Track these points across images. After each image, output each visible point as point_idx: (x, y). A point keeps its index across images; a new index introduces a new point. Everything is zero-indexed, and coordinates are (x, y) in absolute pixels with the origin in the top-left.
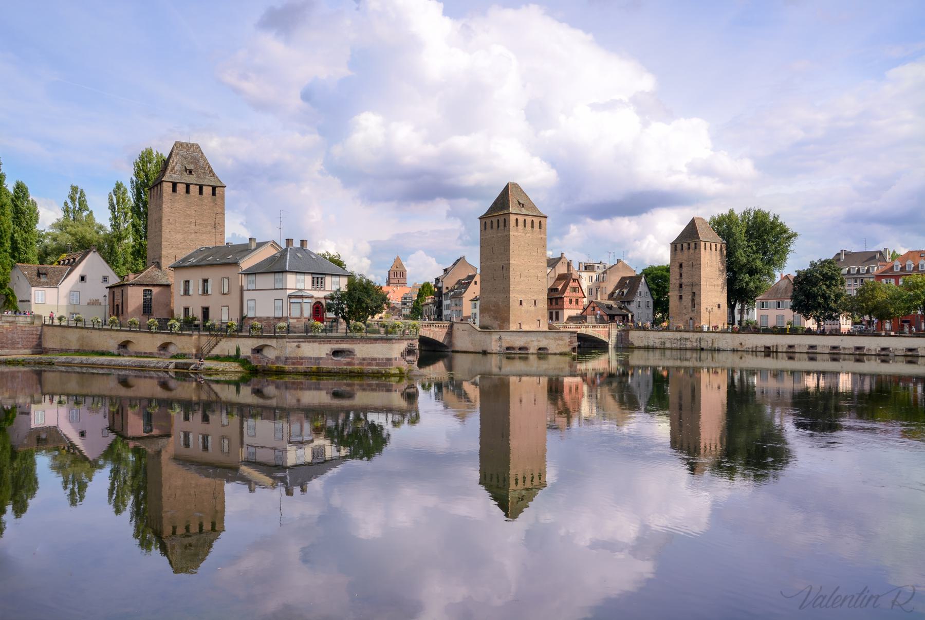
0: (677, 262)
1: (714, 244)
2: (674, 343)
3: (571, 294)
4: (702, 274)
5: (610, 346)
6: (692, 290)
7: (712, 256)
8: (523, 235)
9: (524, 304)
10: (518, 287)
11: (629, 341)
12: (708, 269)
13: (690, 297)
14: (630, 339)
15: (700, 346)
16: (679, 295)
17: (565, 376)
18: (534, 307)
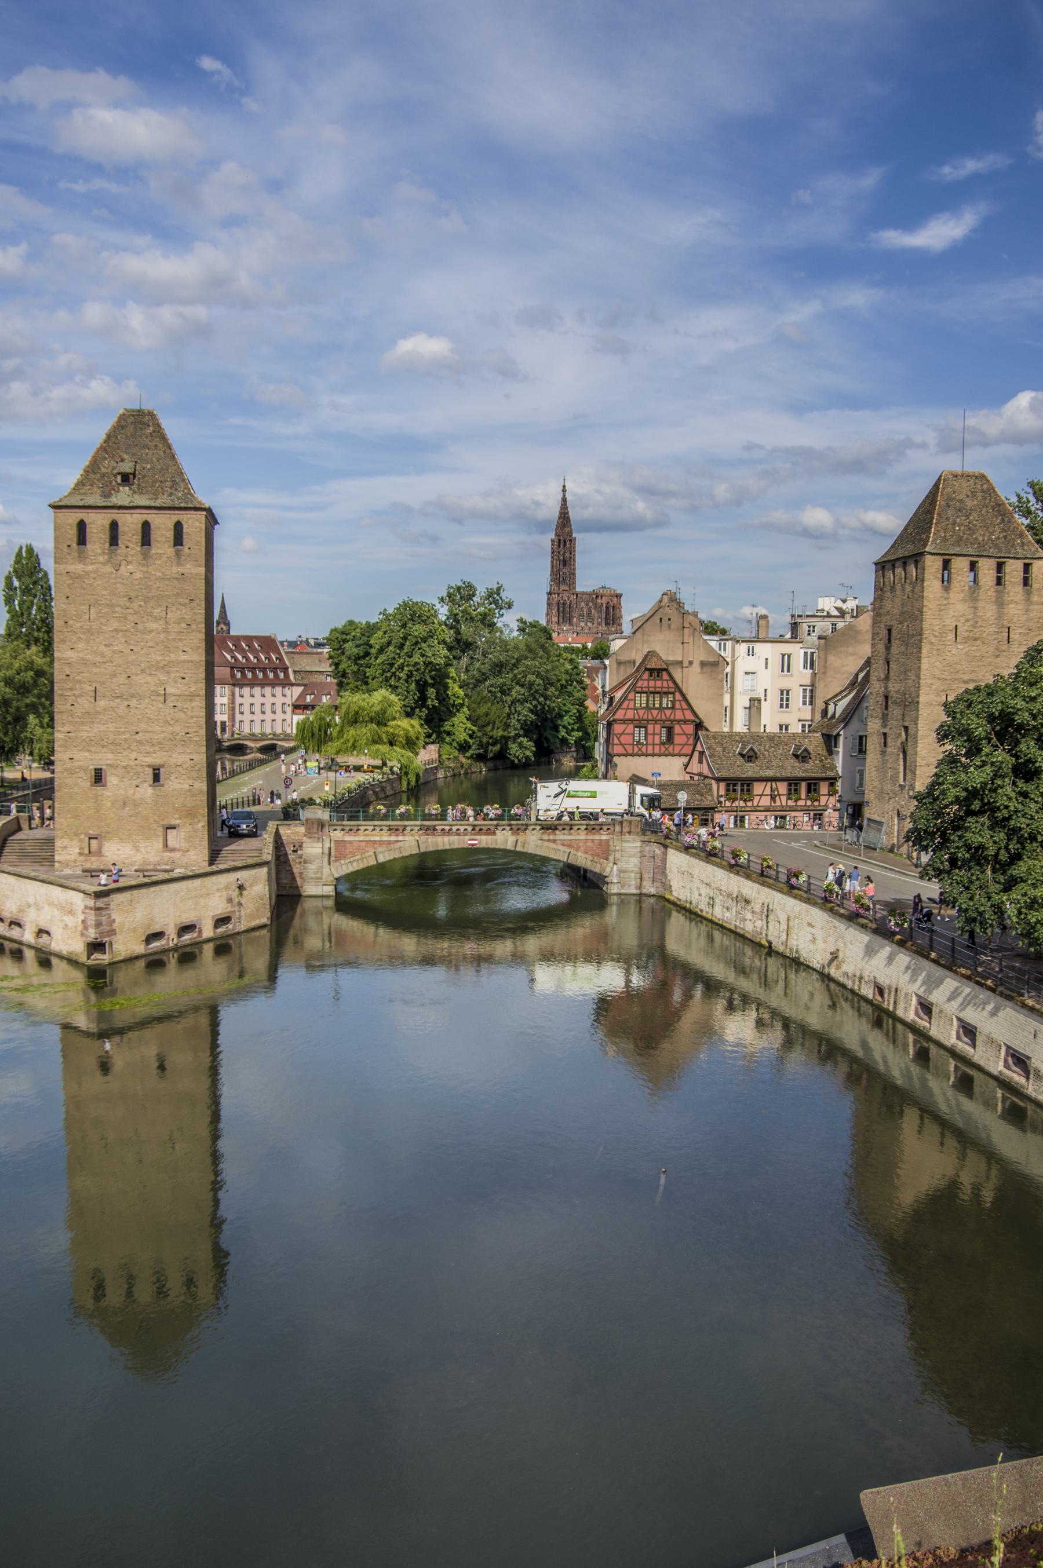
0: (882, 625)
1: (992, 563)
2: (728, 909)
3: (641, 712)
4: (925, 663)
5: (614, 889)
6: (903, 719)
7: (980, 604)
8: (109, 569)
9: (112, 780)
10: (85, 728)
11: (666, 876)
12: (957, 652)
13: (899, 743)
14: (667, 872)
15: (766, 935)
16: (881, 731)
17: (83, 1031)
18: (150, 790)
